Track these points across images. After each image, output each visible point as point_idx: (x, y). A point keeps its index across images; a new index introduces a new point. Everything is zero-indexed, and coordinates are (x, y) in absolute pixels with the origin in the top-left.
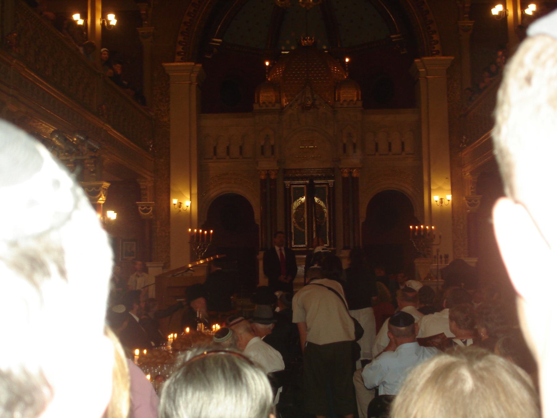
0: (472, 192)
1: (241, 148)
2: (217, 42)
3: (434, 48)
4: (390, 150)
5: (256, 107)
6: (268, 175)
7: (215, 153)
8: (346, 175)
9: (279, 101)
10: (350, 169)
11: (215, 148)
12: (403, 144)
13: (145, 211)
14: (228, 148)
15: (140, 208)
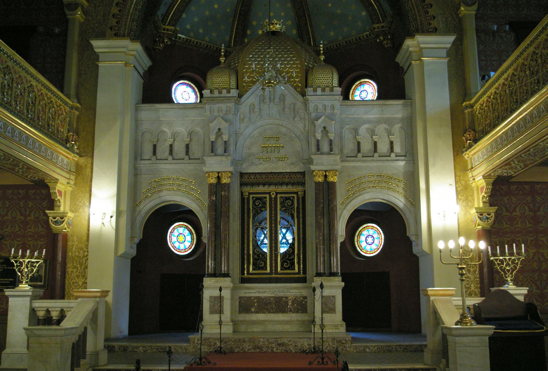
0: (484, 202)
1: (187, 146)
2: (168, 30)
3: (430, 24)
4: (375, 150)
6: (219, 178)
7: (154, 153)
8: (321, 179)
10: (326, 171)
11: (155, 147)
12: (392, 143)
13: (56, 223)
14: (171, 146)
15: (51, 218)
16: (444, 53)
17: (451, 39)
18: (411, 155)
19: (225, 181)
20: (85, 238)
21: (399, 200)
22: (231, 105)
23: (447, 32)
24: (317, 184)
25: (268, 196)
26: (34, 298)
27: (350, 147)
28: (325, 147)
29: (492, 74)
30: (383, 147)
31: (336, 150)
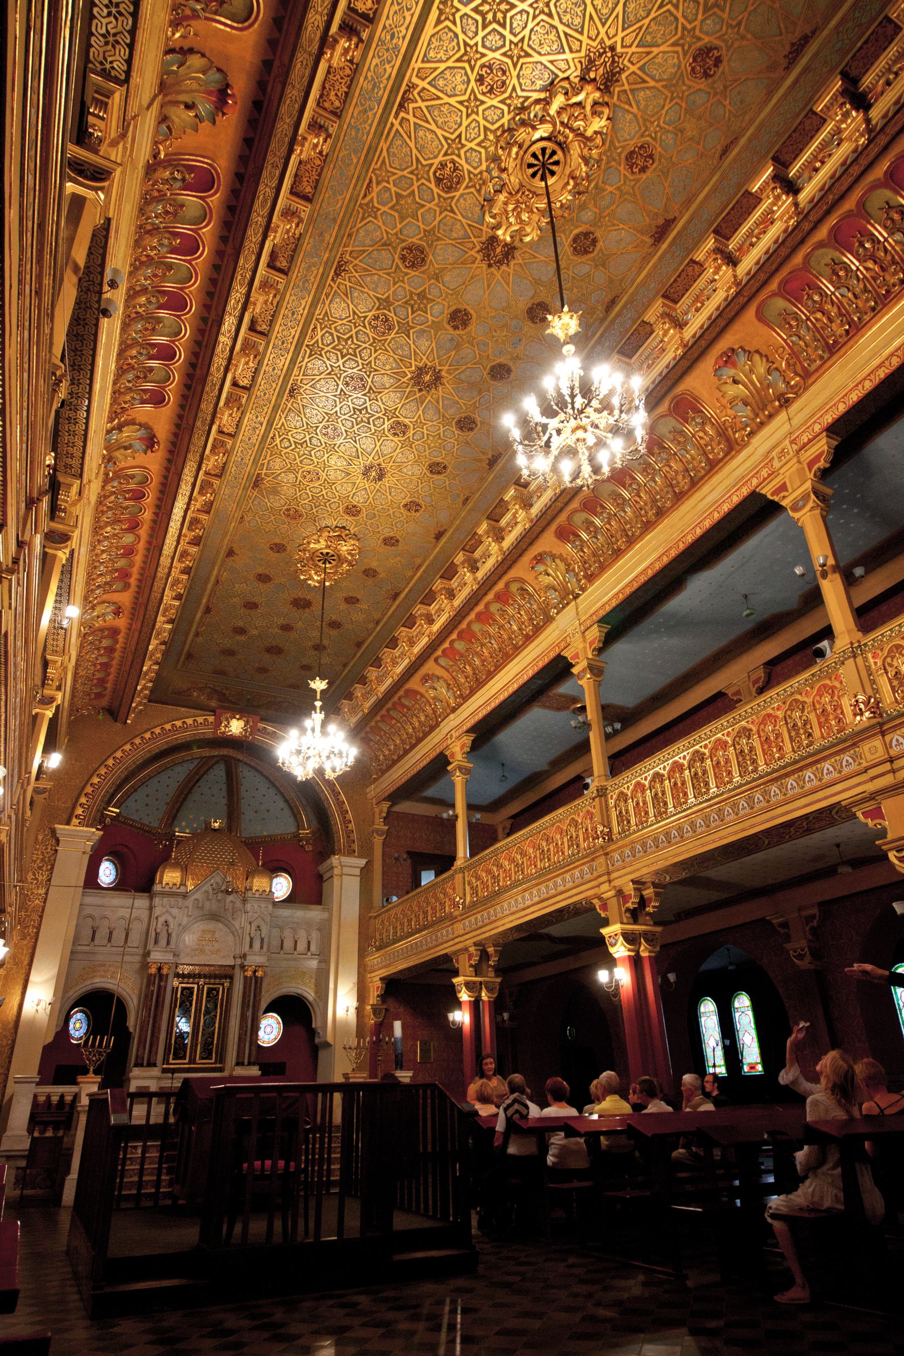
4: (295, 949)
5: (157, 888)
6: (160, 969)
9: (183, 884)
12: (309, 943)
16: (358, 872)
17: (362, 862)
18: (324, 957)
19: (165, 971)
20: (11, 1025)
21: (309, 994)
22: (180, 900)
23: (360, 856)
24: (245, 977)
25: (196, 986)
26: (38, 1084)
27: (276, 943)
28: (257, 945)
29: (395, 899)
30: (302, 946)
31: (265, 947)
